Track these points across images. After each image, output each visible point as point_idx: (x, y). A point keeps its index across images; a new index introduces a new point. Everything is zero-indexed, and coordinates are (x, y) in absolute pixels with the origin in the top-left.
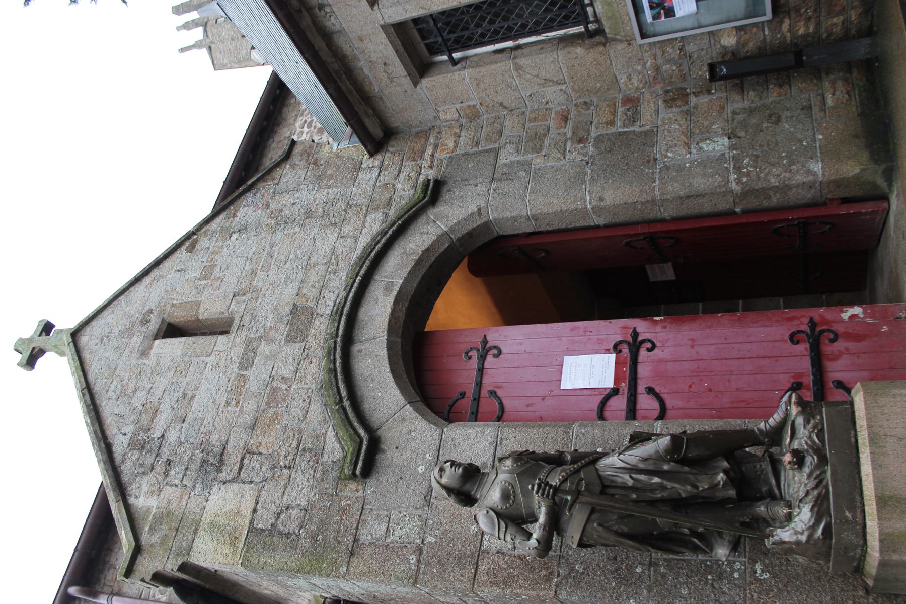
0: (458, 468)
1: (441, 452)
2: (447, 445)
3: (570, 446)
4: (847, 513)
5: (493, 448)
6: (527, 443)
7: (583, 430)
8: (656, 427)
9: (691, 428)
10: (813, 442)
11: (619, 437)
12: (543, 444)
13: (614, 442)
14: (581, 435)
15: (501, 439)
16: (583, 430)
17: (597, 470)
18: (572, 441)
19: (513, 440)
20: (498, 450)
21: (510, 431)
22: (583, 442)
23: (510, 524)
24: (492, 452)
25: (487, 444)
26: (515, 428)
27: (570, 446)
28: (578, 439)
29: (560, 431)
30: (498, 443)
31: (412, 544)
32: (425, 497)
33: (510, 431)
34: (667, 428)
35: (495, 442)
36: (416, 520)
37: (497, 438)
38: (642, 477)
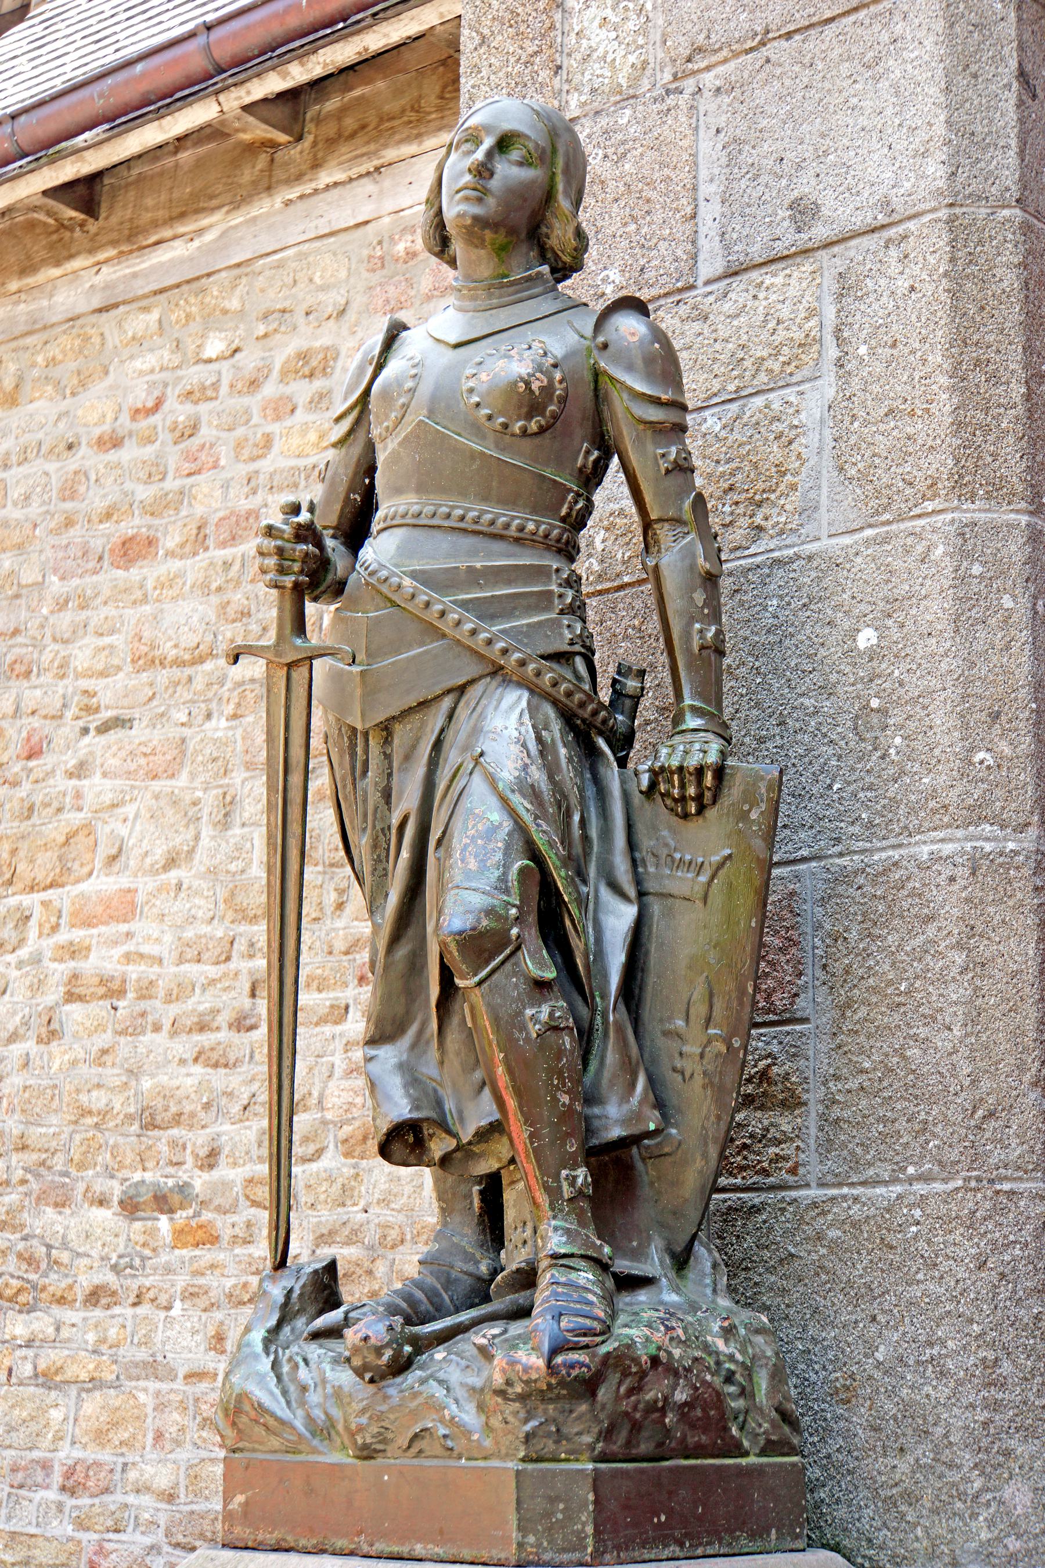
0: (467, 199)
1: (852, 18)
2: (877, 27)
3: (886, 517)
4: (240, 1498)
5: (869, 220)
6: (894, 345)
7: (940, 550)
8: (960, 833)
9: (954, 971)
10: (415, 1415)
11: (914, 701)
12: (891, 411)
13: (901, 684)
14: (920, 549)
15: (905, 237)
16: (940, 550)
17: (461, 690)
18: (900, 519)
19: (903, 284)
20: (865, 242)
21: (932, 260)
22: (898, 564)
23: (356, 449)
24: (860, 220)
25: (883, 190)
26: (946, 274)
27: (886, 517)
28: (909, 541)
29: (941, 463)
30: (892, 232)
31: (566, 87)
32: (700, 50)
33: (932, 260)
34: (952, 879)
35: (896, 217)
36: (632, 59)
37: (910, 218)
38: (405, 854)
